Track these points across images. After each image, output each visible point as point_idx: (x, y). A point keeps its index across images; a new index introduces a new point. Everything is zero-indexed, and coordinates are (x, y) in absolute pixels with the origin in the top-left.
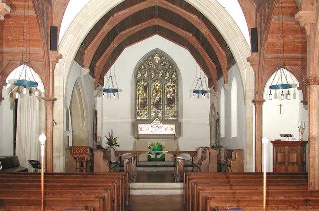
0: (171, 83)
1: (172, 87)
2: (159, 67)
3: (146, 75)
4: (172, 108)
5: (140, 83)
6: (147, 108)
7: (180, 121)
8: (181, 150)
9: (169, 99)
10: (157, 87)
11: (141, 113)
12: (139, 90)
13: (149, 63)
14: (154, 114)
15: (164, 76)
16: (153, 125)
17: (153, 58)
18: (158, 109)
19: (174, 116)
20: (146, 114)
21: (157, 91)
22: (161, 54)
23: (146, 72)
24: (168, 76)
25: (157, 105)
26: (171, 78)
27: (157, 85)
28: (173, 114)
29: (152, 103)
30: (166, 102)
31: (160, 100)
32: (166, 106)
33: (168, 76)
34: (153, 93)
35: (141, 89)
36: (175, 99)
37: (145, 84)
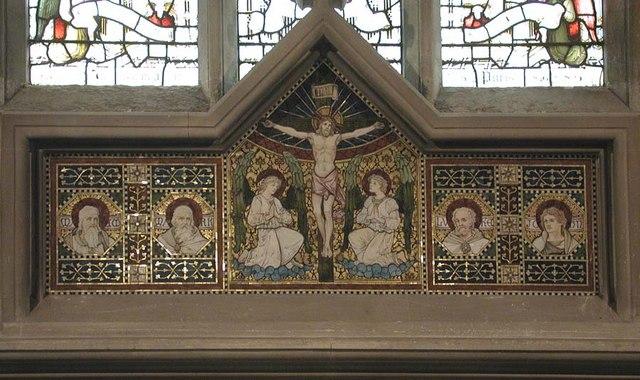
19: (563, 42)
20: (168, 21)
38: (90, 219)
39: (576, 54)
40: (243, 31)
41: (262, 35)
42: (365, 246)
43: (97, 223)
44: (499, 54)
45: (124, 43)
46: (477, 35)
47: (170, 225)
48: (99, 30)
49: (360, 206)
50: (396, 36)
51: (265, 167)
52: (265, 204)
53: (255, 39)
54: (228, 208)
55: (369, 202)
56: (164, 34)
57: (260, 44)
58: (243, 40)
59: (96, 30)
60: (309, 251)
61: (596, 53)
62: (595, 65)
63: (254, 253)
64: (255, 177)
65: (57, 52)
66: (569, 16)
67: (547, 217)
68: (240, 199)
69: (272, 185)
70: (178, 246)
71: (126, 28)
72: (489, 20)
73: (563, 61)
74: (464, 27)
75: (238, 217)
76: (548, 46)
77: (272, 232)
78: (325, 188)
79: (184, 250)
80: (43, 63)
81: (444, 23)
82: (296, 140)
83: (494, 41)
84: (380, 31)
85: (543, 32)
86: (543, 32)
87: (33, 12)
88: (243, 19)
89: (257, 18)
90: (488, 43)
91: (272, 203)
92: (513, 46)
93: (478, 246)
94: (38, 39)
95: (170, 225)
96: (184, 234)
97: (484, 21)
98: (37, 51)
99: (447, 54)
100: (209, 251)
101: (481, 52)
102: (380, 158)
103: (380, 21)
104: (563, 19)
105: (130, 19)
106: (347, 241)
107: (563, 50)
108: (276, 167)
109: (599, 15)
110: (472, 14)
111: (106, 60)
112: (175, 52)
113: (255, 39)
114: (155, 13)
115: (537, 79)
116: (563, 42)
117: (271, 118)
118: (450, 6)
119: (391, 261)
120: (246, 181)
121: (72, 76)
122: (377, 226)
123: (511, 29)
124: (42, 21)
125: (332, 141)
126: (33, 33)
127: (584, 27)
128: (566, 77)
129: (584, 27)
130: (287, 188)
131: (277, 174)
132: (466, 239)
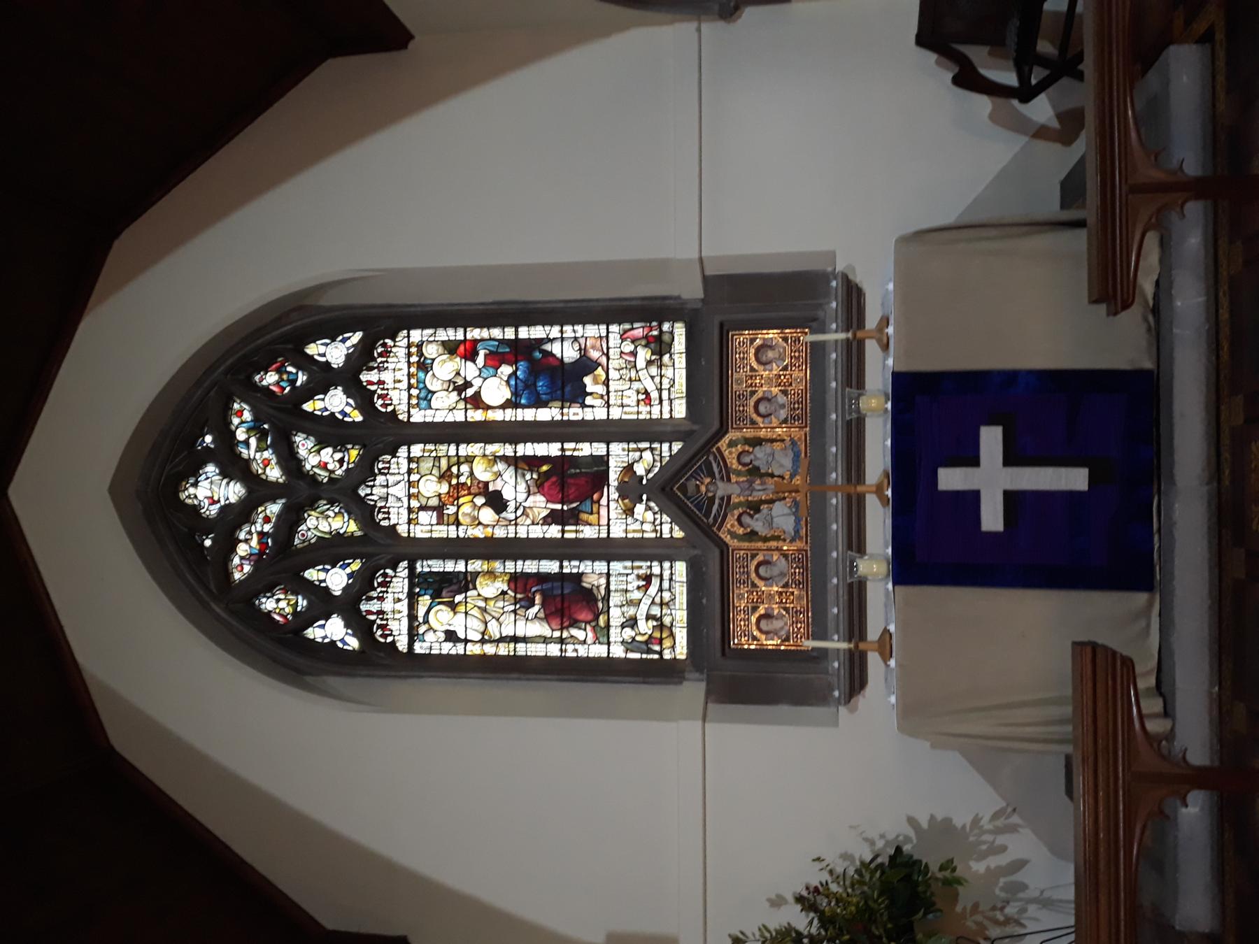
1: (424, 366)
2: (274, 473)
3: (336, 580)
4: (585, 365)
5: (399, 631)
6: (592, 571)
7: (692, 290)
10: (431, 488)
11: (632, 622)
12: (451, 636)
13: (242, 549)
14: (639, 508)
16: (731, 522)
17: (207, 525)
18: (601, 479)
19: (660, 347)
20: (648, 579)
21: (457, 491)
23: (312, 574)
24: (336, 402)
26: (348, 378)
28: (644, 354)
29: (554, 531)
30: (544, 414)
31: (532, 462)
32: (575, 413)
33: (336, 402)
35: (442, 618)
36: (516, 342)
37: (400, 584)
38: (767, 625)
39: (666, 338)
40: (653, 535)
41: (656, 523)
42: (782, 466)
43: (770, 620)
44: (666, 385)
45: (661, 604)
46: (654, 395)
47: (770, 578)
48: (654, 618)
49: (757, 469)
50: (656, 445)
51: (736, 523)
52: (757, 525)
53: (658, 528)
54: (760, 544)
55: (756, 463)
57: (661, 524)
58: (658, 535)
59: (576, 638)
60: (784, 498)
61: (666, 327)
62: (673, 327)
63: (786, 530)
64: (742, 529)
65: (667, 643)
66: (643, 342)
67: (764, 359)
68: (755, 538)
69: (746, 519)
70: (782, 574)
71: (653, 603)
72: (646, 390)
73: (670, 345)
74: (651, 406)
75: (765, 539)
76: (661, 356)
77: (775, 520)
78: (748, 488)
79: (785, 571)
80: (674, 651)
81: (648, 417)
82: (720, 506)
83: (659, 387)
84: (653, 455)
85: (653, 357)
86: (653, 357)
87: (644, 656)
88: (646, 535)
89: (647, 527)
90: (660, 390)
91: (757, 520)
92: (661, 377)
93: (782, 399)
94: (660, 653)
95: (770, 578)
96: (775, 571)
97: (647, 393)
98: (667, 655)
99: (666, 416)
100: (786, 556)
101: (665, 395)
102: (730, 456)
103: (647, 455)
104: (646, 346)
105: (646, 602)
106: (779, 476)
107: (663, 346)
108: (736, 517)
109: (643, 324)
110: (642, 400)
111: (671, 614)
112: (666, 574)
113: (658, 528)
114: (643, 586)
115: (681, 362)
116: (660, 347)
117: (708, 519)
118: (638, 413)
119: (790, 451)
120: (744, 534)
121: (681, 636)
122: (770, 459)
123: (652, 377)
124: (650, 651)
125: (720, 484)
126: (656, 656)
127: (650, 334)
128: (680, 344)
129: (650, 334)
130: (748, 511)
131: (740, 515)
132: (777, 407)
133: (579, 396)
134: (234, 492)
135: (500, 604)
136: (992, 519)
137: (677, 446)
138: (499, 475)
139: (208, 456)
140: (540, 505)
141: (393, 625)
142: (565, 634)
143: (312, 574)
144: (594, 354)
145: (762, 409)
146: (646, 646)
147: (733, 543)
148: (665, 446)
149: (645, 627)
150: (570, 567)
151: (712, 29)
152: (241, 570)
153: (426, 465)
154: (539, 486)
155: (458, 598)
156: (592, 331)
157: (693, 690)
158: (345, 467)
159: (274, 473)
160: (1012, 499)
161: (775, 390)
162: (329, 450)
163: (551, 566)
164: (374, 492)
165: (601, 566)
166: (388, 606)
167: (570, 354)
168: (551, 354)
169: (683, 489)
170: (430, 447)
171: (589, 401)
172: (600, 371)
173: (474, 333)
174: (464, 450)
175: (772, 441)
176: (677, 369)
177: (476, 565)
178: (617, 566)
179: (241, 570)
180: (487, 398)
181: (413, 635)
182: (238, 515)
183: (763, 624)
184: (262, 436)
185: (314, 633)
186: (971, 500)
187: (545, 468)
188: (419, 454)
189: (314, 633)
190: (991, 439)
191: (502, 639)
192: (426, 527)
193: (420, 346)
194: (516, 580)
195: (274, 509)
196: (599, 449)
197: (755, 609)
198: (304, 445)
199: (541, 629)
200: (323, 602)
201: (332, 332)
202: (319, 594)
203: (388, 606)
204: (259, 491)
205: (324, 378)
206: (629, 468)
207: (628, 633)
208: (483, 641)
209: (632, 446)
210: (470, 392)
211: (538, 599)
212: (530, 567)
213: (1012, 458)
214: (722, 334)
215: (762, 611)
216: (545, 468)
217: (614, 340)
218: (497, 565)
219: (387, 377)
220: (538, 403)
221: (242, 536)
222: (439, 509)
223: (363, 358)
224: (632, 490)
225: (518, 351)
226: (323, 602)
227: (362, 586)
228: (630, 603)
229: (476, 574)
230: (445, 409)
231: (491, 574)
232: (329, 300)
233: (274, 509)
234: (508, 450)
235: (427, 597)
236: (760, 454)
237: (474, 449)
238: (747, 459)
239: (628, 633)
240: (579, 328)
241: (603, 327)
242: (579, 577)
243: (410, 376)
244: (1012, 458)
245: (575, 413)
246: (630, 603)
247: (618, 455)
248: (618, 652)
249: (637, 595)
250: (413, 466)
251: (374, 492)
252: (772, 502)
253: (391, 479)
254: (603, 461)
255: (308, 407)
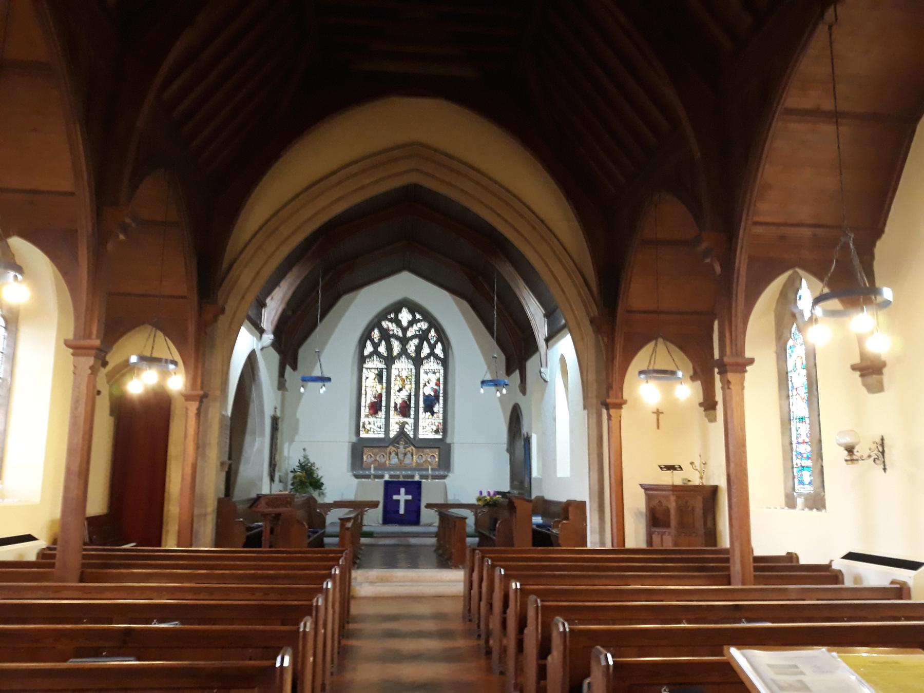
0: (431, 365)
1: (434, 373)
2: (409, 334)
3: (382, 349)
4: (433, 413)
6: (382, 414)
7: (448, 441)
8: (450, 502)
9: (427, 398)
10: (404, 374)
13: (390, 324)
15: (419, 348)
16: (394, 449)
19: (437, 432)
20: (380, 428)
22: (414, 308)
23: (383, 343)
24: (426, 350)
25: (404, 409)
27: (403, 367)
28: (435, 428)
31: (409, 399)
34: (395, 385)
46: (425, 430)
50: (412, 431)
52: (393, 455)
56: (379, 430)
61: (441, 433)
75: (389, 457)
93: (422, 461)
98: (361, 432)
101: (424, 433)
116: (437, 432)
133: (426, 411)
134: (405, 324)
135: (375, 391)
136: (395, 497)
137: (412, 436)
138: (407, 391)
139: (414, 316)
140: (399, 402)
141: (370, 363)
142: (367, 407)
143: (383, 343)
144: (435, 415)
145: (420, 457)
146: (364, 427)
147: (388, 449)
148: (412, 433)
149: (368, 427)
150: (383, 408)
151: (505, 446)
152: (385, 324)
153: (410, 373)
154: (404, 402)
155: (377, 380)
156: (441, 415)
157: (354, 439)
158: (410, 352)
159: (409, 334)
160: (398, 501)
161: (424, 460)
162: (414, 348)
163: (384, 404)
164: (404, 358)
165: (383, 416)
166: (375, 362)
167: (436, 409)
168: (436, 404)
169: (402, 437)
170: (414, 374)
171: (424, 414)
172: (431, 417)
173: (442, 386)
174: (413, 383)
175: (412, 458)
176: (432, 436)
177: (385, 385)
178: (383, 420)
179: (385, 324)
180: (426, 387)
181: (367, 368)
182: (398, 323)
183: (369, 456)
184: (419, 331)
185: (368, 343)
186: (398, 493)
187: (408, 403)
188: (412, 371)
189: (368, 343)
190: (409, 497)
191: (366, 390)
192: (394, 373)
193: (439, 372)
194: (380, 395)
195: (400, 334)
196: (412, 416)
197: (373, 454)
198: (416, 341)
199: (368, 402)
200: (376, 346)
201: (445, 350)
202: (379, 344)
203: (375, 362)
204: (404, 330)
205: (432, 347)
206: (407, 423)
207: (367, 423)
208: (366, 386)
209: (413, 425)
210: (427, 384)
211: (376, 400)
212: (384, 399)
213: (406, 501)
214: (438, 448)
215: (372, 455)
216: (408, 403)
217: (439, 421)
218: (384, 390)
219: (432, 363)
220: (425, 401)
221: (394, 324)
222: (399, 376)
223: (437, 357)
224: (402, 426)
225: (437, 397)
226: (376, 346)
227: (379, 355)
228: (374, 423)
229: (382, 385)
230: (423, 378)
231: (382, 388)
232: (450, 352)
233: (400, 334)
234: (413, 394)
235: (377, 373)
236: (409, 455)
237: (413, 386)
238: (408, 453)
239: (367, 423)
240: (442, 412)
241: (442, 418)
242: (381, 410)
243: (432, 370)
244: (406, 501)
245: (421, 410)
246: (374, 423)
247: (410, 421)
248: (362, 420)
249: (376, 425)
250: (410, 370)
251: (404, 358)
252: (398, 458)
253: (407, 364)
254: (409, 416)
255: (425, 343)
